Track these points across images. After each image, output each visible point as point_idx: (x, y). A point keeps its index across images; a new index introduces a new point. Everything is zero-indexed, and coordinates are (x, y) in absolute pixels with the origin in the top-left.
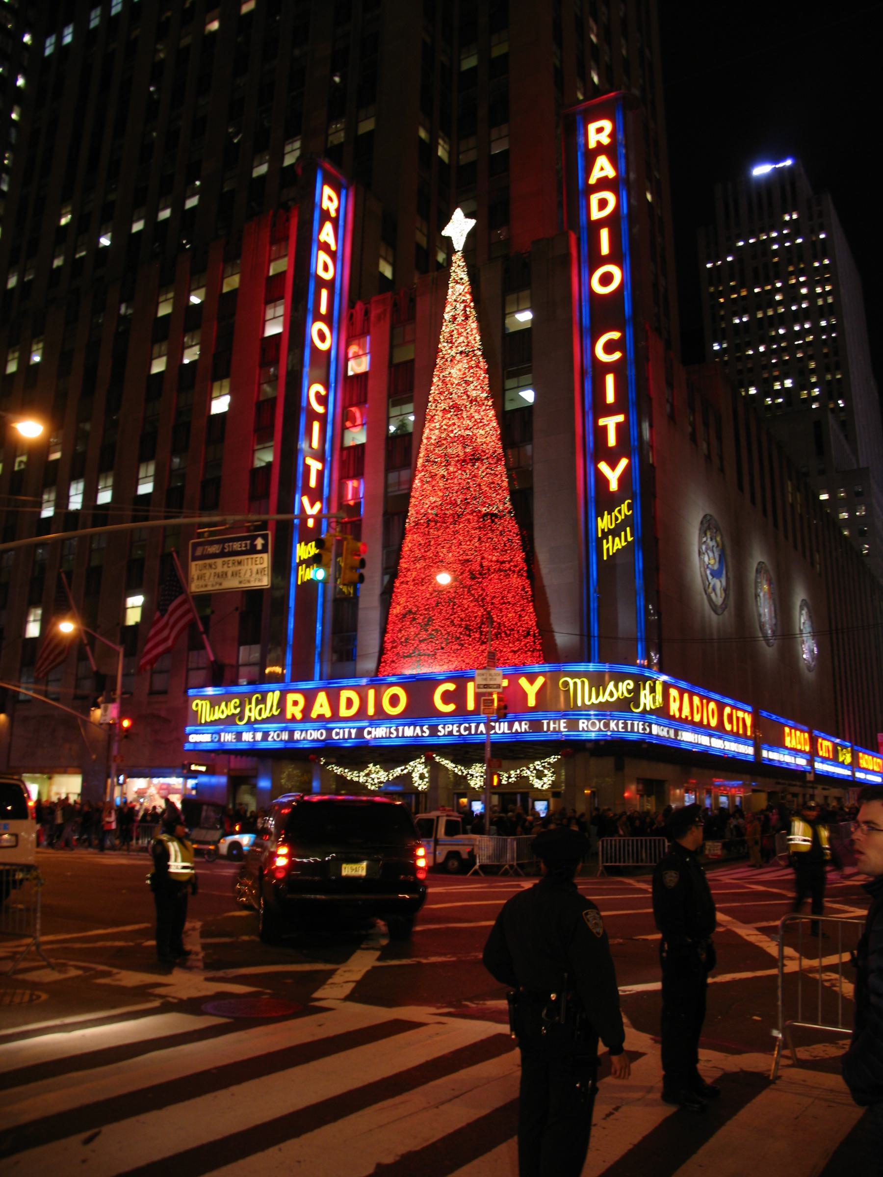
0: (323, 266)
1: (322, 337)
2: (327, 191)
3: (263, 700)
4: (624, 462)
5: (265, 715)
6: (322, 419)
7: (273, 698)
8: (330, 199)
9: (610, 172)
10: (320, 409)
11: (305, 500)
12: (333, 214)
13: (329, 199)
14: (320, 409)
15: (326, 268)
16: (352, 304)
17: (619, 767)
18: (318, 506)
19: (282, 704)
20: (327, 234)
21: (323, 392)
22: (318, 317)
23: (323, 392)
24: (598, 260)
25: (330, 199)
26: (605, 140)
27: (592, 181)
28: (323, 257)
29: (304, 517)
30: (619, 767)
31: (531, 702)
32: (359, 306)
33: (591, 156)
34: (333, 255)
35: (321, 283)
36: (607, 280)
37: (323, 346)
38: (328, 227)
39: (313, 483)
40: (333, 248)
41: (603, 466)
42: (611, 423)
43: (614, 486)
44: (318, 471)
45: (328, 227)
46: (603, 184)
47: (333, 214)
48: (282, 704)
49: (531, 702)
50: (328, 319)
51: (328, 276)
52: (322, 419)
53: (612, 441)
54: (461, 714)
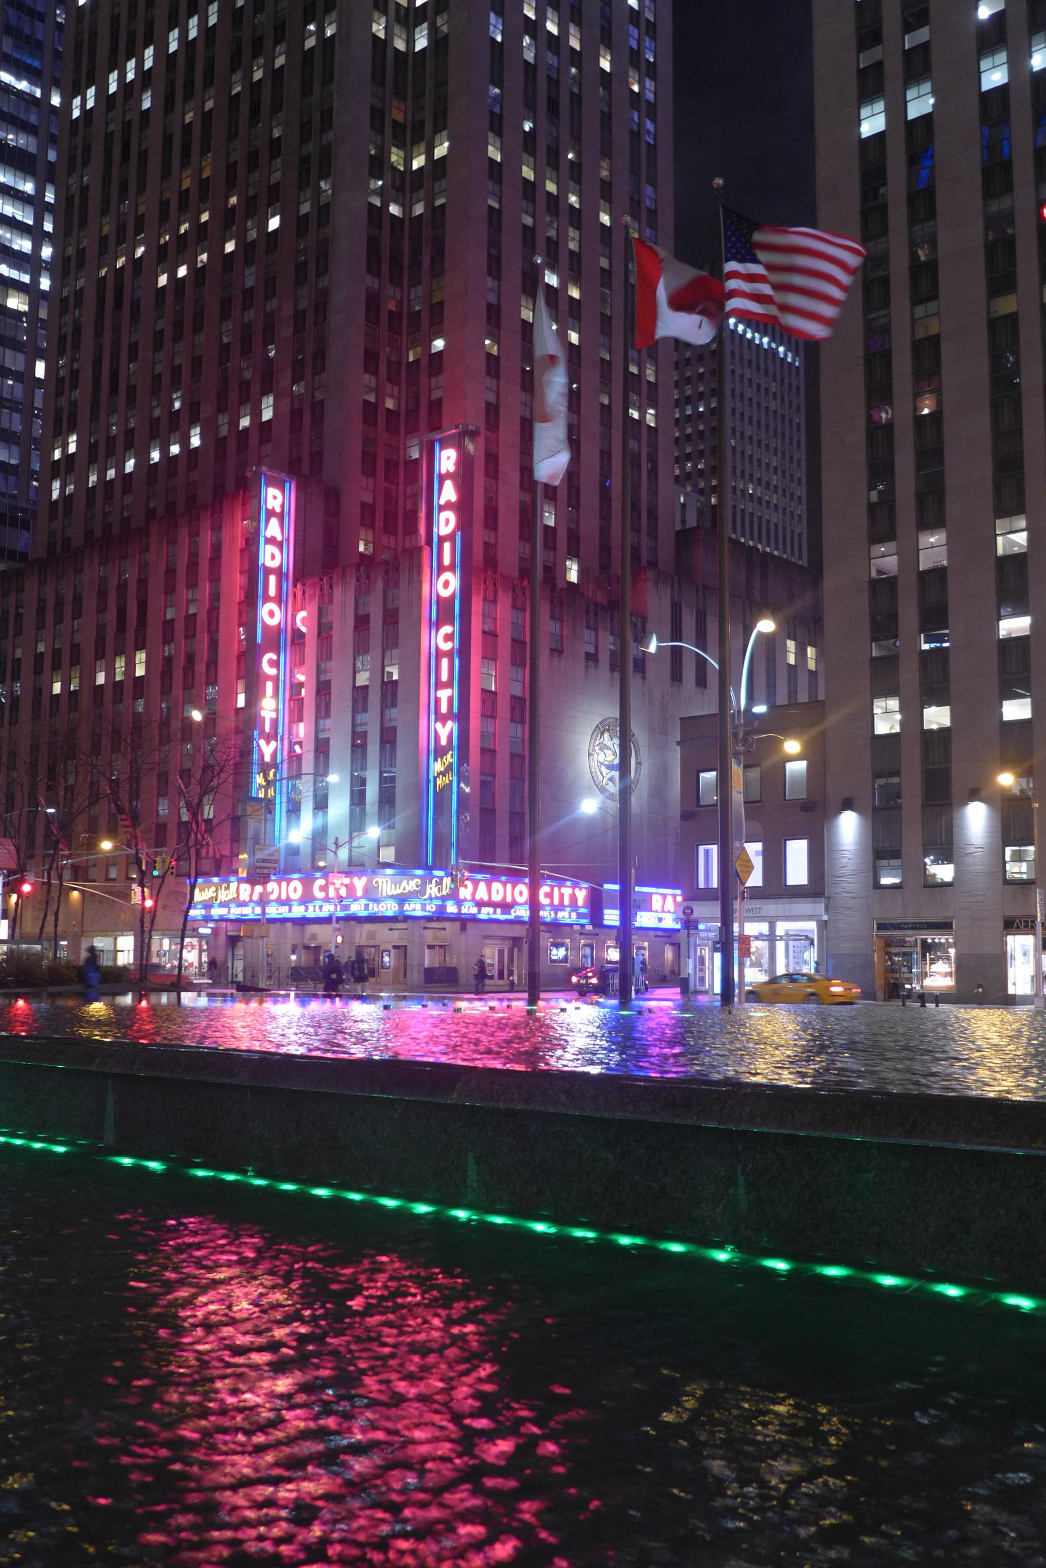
0: (270, 557)
1: (271, 614)
2: (272, 491)
3: (227, 888)
4: (450, 724)
5: (230, 897)
6: (276, 679)
7: (233, 886)
8: (275, 497)
9: (453, 498)
10: (272, 672)
11: (262, 742)
12: (278, 510)
13: (273, 498)
14: (273, 672)
15: (273, 557)
16: (295, 586)
17: (463, 928)
18: (273, 744)
19: (238, 891)
20: (273, 529)
21: (274, 657)
22: (267, 599)
23: (274, 657)
24: (441, 569)
25: (275, 497)
26: (452, 469)
27: (442, 502)
28: (271, 549)
29: (262, 755)
30: (463, 928)
31: (359, 893)
32: (299, 586)
33: (442, 478)
34: (279, 545)
35: (268, 571)
36: (448, 585)
37: (273, 622)
38: (274, 522)
39: (267, 729)
40: (279, 538)
41: (439, 725)
42: (444, 694)
43: (444, 742)
44: (272, 720)
45: (274, 522)
46: (449, 506)
47: (278, 510)
48: (238, 891)
49: (359, 893)
50: (278, 600)
51: (275, 564)
52: (276, 679)
53: (444, 709)
54: (327, 899)
